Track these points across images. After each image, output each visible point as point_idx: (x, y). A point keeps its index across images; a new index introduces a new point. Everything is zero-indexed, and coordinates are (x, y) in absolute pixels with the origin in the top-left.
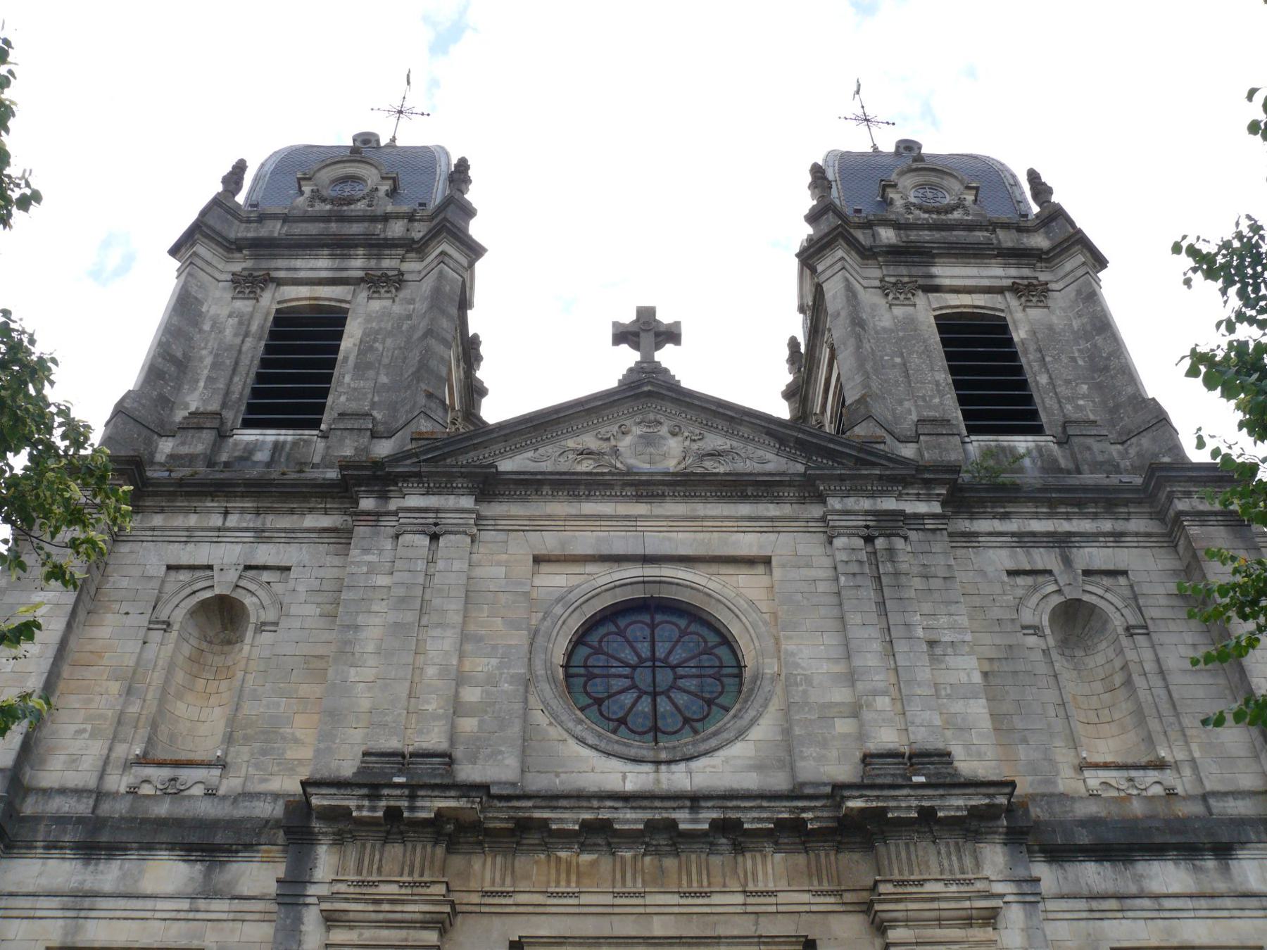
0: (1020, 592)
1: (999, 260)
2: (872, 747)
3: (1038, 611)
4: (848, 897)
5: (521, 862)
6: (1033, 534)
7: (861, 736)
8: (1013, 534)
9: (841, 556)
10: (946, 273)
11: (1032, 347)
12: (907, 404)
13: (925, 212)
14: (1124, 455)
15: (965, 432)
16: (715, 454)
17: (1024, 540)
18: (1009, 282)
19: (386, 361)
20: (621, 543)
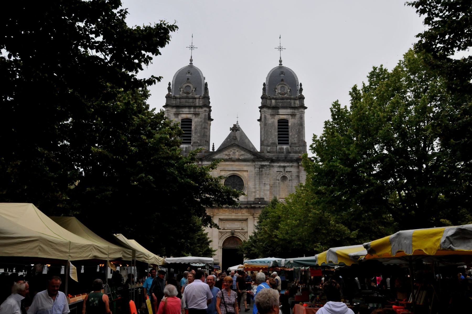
0: (277, 174)
2: (256, 197)
3: (279, 178)
4: (252, 214)
5: (220, 210)
6: (281, 166)
7: (255, 196)
8: (278, 166)
9: (256, 171)
10: (281, 111)
11: (291, 127)
12: (270, 139)
13: (281, 95)
14: (298, 149)
15: (277, 144)
16: (242, 155)
17: (280, 167)
19: (199, 131)
20: (230, 168)
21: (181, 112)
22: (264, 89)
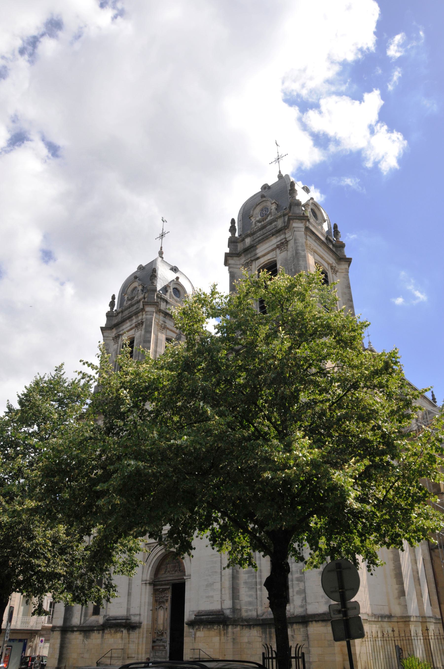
1: (274, 236)
18: (275, 246)
21: (121, 333)
22: (232, 229)
